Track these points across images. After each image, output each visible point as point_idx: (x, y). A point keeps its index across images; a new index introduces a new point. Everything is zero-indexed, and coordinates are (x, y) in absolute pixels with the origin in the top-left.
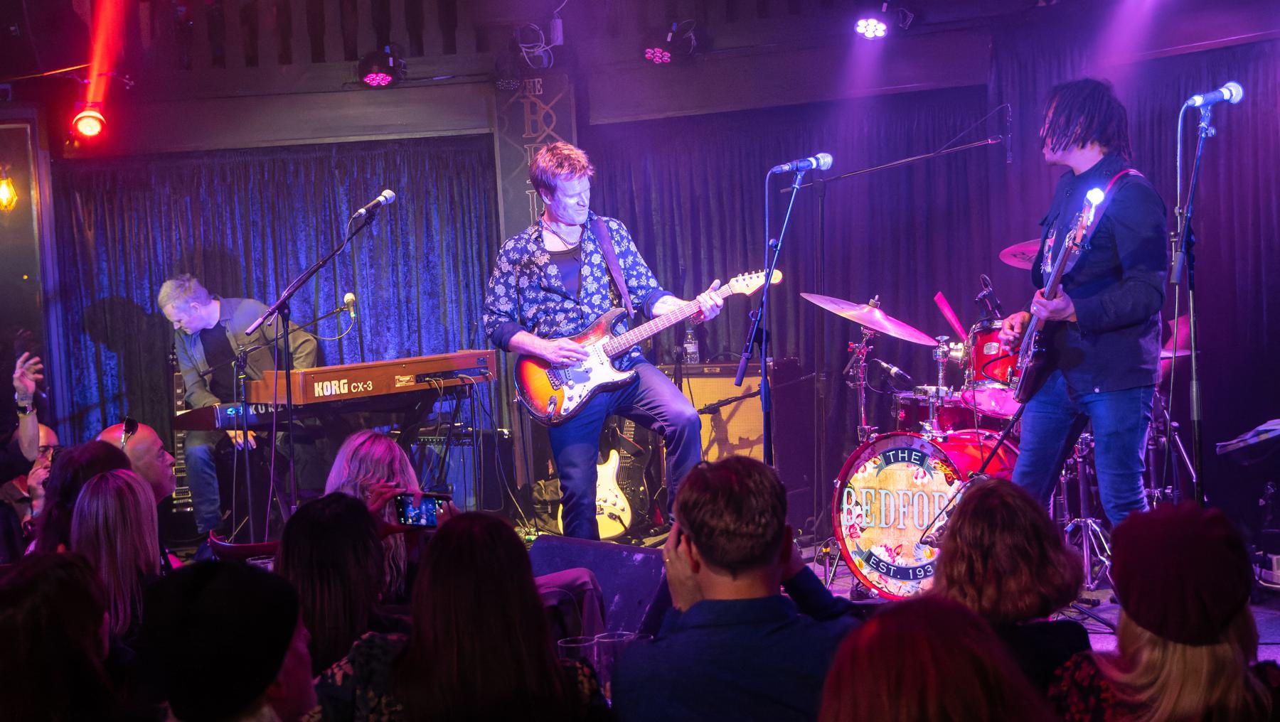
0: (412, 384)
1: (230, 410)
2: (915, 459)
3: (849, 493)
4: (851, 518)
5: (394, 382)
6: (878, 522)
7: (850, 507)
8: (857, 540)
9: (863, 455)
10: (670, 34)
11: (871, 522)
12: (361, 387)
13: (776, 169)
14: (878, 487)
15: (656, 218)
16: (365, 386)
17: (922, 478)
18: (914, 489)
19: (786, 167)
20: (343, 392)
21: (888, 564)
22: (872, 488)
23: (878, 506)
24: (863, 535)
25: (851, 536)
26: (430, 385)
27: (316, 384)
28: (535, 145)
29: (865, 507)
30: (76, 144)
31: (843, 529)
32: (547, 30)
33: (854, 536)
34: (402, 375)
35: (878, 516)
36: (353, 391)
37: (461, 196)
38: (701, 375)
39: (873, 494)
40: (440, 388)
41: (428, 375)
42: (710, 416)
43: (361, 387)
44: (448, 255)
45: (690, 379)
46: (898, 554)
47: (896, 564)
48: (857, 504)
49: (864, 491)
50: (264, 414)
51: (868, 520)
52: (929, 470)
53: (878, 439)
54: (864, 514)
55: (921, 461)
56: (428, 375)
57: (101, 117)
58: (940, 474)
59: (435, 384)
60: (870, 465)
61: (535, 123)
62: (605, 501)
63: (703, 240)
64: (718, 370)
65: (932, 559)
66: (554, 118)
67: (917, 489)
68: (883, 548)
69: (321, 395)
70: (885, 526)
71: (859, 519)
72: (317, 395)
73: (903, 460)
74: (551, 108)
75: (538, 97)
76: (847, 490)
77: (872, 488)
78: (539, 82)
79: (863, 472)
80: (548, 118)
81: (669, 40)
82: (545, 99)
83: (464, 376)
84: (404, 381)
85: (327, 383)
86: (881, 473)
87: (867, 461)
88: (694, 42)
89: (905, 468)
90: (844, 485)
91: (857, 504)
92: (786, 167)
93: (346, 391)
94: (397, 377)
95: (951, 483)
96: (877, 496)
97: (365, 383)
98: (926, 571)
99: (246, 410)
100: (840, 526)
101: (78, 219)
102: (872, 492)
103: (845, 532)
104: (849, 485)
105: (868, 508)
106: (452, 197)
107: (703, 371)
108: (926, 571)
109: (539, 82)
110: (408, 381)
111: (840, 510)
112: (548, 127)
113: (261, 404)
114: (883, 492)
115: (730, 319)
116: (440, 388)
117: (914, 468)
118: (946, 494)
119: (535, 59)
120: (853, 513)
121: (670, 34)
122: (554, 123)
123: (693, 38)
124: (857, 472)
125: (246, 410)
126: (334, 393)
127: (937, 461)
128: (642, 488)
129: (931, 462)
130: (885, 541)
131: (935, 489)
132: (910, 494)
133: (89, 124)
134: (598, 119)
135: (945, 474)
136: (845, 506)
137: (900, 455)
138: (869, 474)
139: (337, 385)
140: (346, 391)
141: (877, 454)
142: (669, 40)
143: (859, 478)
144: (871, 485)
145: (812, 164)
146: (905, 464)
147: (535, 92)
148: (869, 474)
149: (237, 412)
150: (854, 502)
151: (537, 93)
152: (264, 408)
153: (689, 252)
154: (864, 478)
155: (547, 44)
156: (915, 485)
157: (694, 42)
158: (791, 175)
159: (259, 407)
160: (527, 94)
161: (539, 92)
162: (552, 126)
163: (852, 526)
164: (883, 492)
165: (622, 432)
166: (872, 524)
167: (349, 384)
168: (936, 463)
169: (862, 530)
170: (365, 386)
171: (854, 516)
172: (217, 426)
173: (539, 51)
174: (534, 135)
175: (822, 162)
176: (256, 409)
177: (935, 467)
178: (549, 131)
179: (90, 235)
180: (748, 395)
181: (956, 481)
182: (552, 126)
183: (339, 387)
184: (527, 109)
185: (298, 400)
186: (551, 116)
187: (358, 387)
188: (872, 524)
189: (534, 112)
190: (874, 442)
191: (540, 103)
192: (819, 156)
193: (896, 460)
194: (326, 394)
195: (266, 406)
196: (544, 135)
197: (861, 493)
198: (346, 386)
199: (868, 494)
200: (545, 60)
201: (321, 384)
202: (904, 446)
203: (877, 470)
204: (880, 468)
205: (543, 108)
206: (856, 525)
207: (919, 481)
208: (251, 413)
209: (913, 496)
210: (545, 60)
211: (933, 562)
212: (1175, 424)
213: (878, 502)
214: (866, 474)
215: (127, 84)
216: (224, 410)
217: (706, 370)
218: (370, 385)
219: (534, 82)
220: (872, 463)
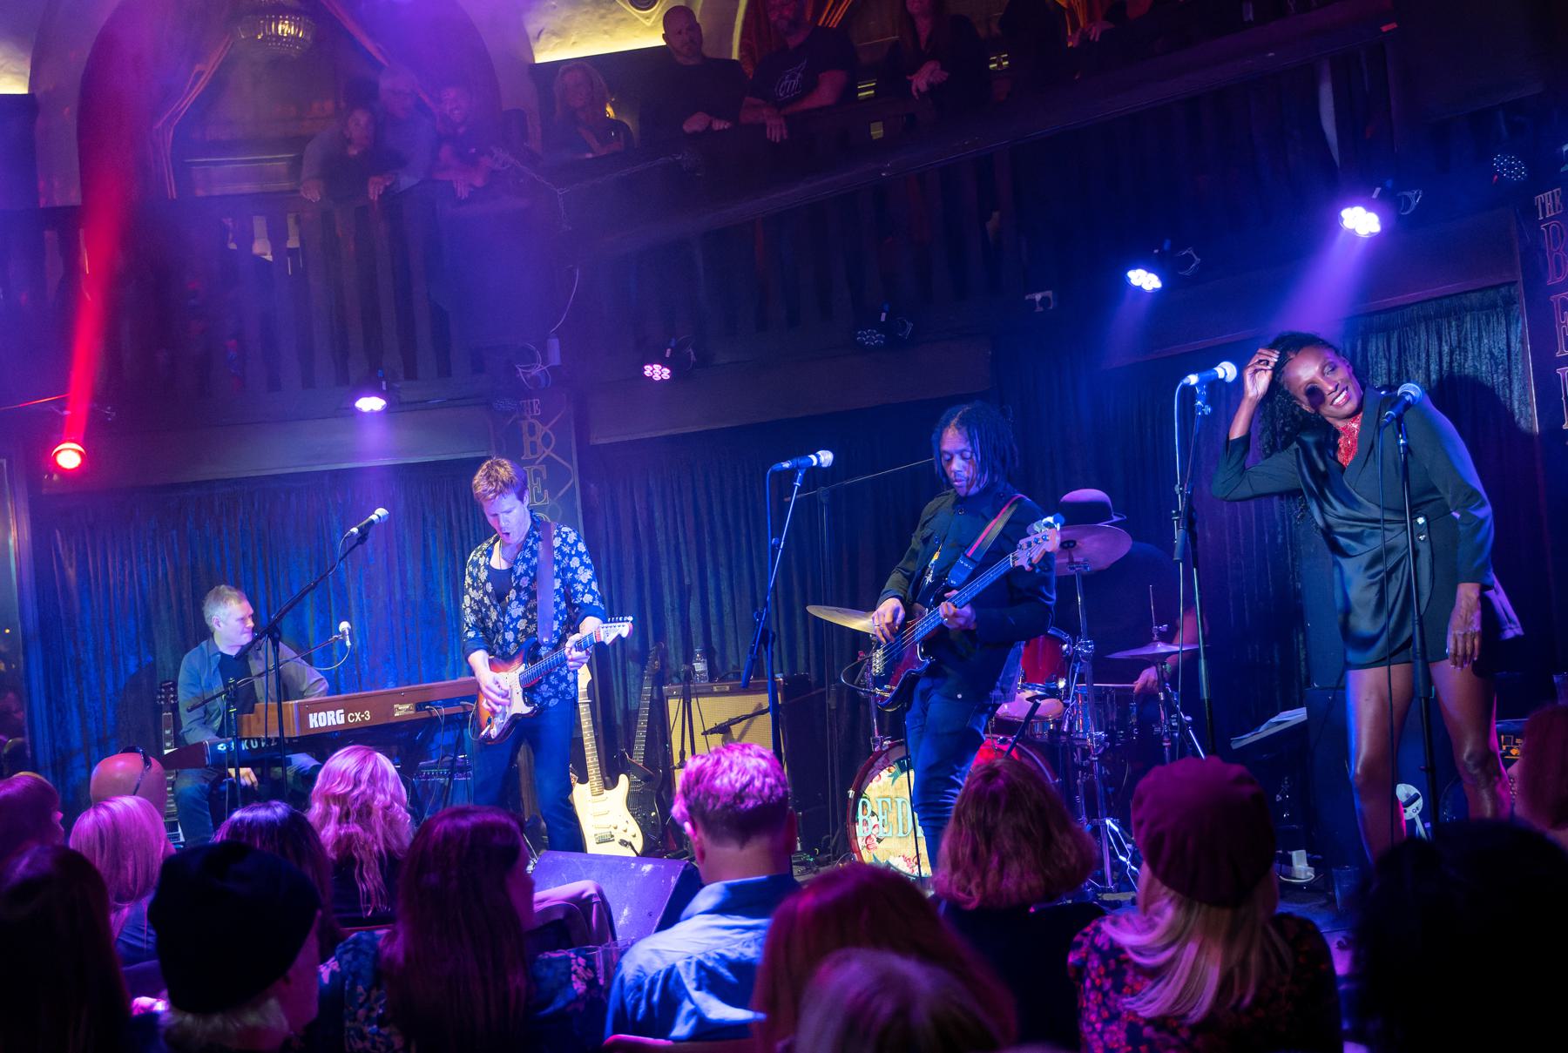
0: (412, 712)
1: (222, 745)
3: (864, 803)
4: (867, 829)
5: (393, 711)
6: (895, 832)
7: (866, 817)
8: (875, 852)
9: (876, 764)
10: (669, 350)
12: (358, 718)
13: (776, 467)
14: (892, 794)
15: (661, 538)
16: (363, 716)
19: (786, 465)
20: (339, 722)
22: (888, 797)
23: (895, 815)
24: (881, 846)
25: (867, 847)
26: (430, 712)
27: (311, 715)
28: (535, 467)
30: (55, 477)
31: (859, 840)
32: (544, 349)
33: (870, 847)
34: (402, 703)
35: (895, 826)
36: (349, 720)
37: (459, 521)
38: (711, 694)
40: (442, 716)
41: (429, 703)
42: (720, 736)
43: (358, 718)
44: (447, 582)
45: (699, 699)
48: (873, 814)
49: (880, 801)
50: (256, 749)
51: (885, 830)
53: (891, 746)
54: (880, 823)
56: (429, 703)
57: (82, 450)
59: (435, 712)
60: (885, 774)
61: (533, 444)
62: (616, 828)
63: (708, 557)
64: (728, 688)
66: (552, 435)
68: (901, 858)
69: (316, 726)
70: (902, 835)
71: (876, 829)
72: (312, 726)
74: (550, 429)
75: (536, 418)
76: (862, 800)
77: (888, 797)
78: (537, 402)
79: (877, 781)
80: (546, 438)
81: (668, 355)
82: (544, 419)
83: (466, 703)
84: (403, 710)
85: (322, 714)
86: (897, 781)
87: (882, 770)
88: (693, 358)
90: (859, 795)
91: (873, 814)
92: (786, 465)
93: (343, 722)
94: (395, 706)
96: (894, 805)
97: (362, 713)
99: (238, 746)
100: (856, 838)
101: (58, 557)
102: (888, 800)
103: (861, 843)
104: (864, 795)
105: (885, 817)
106: (450, 523)
107: (712, 689)
109: (537, 402)
110: (407, 710)
111: (855, 821)
112: (547, 448)
113: (253, 739)
114: (899, 801)
115: (739, 637)
116: (442, 716)
119: (535, 380)
120: (869, 822)
121: (669, 350)
122: (553, 443)
123: (692, 353)
124: (871, 781)
125: (238, 746)
126: (329, 724)
128: (653, 814)
130: (902, 853)
133: (69, 457)
134: (598, 439)
136: (860, 817)
138: (884, 783)
139: (333, 716)
140: (343, 722)
141: (891, 763)
142: (668, 355)
143: (873, 788)
144: (887, 794)
145: (812, 462)
147: (532, 411)
148: (884, 783)
149: (229, 749)
150: (869, 812)
151: (535, 414)
152: (256, 743)
153: (695, 572)
154: (879, 787)
155: (544, 363)
157: (693, 358)
158: (791, 473)
159: (252, 742)
160: (526, 414)
161: (537, 412)
162: (552, 446)
163: (869, 837)
164: (899, 801)
165: (631, 756)
166: (890, 834)
167: (346, 714)
169: (879, 840)
170: (363, 716)
171: (870, 827)
172: (207, 763)
173: (534, 372)
174: (533, 457)
175: (822, 459)
176: (249, 744)
178: (548, 452)
179: (71, 573)
180: (760, 712)
182: (552, 446)
183: (335, 717)
184: (525, 428)
185: (292, 731)
186: (551, 439)
187: (355, 717)
188: (890, 834)
189: (532, 431)
190: (887, 750)
191: (538, 426)
192: (819, 453)
194: (323, 724)
195: (259, 740)
196: (544, 456)
198: (343, 716)
199: (885, 805)
200: (543, 381)
201: (315, 714)
203: (892, 778)
204: (895, 777)
205: (541, 429)
206: (873, 836)
208: (243, 748)
210: (543, 381)
212: (1189, 718)
213: (894, 811)
214: (881, 783)
215: (109, 416)
216: (214, 745)
217: (715, 689)
218: (368, 715)
219: (532, 403)
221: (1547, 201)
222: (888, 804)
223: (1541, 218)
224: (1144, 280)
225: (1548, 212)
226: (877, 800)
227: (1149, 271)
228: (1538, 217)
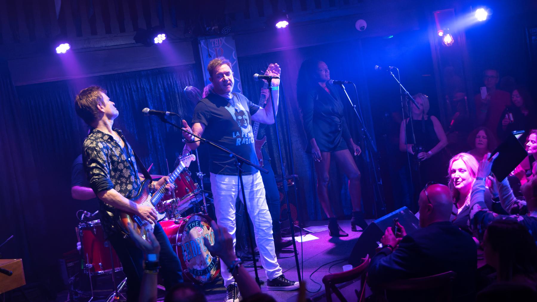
2: (197, 224)
11: (191, 256)
17: (201, 231)
18: (200, 236)
21: (200, 271)
22: (187, 242)
29: (187, 251)
39: (189, 244)
46: (201, 265)
47: (202, 269)
48: (185, 251)
49: (185, 244)
52: (202, 227)
54: (188, 254)
55: (199, 225)
58: (205, 228)
65: (211, 261)
67: (200, 236)
73: (194, 226)
77: (187, 242)
89: (195, 229)
95: (209, 229)
98: (211, 267)
102: (188, 243)
108: (211, 267)
117: (198, 228)
118: (208, 234)
127: (203, 222)
129: (202, 223)
131: (205, 233)
132: (199, 239)
135: (207, 226)
137: (193, 225)
144: (187, 241)
146: (195, 227)
156: (199, 235)
168: (203, 223)
169: (189, 261)
177: (203, 225)
181: (210, 228)
188: (191, 257)
193: (192, 227)
197: (185, 245)
202: (193, 220)
203: (187, 234)
206: (187, 260)
207: (200, 233)
209: (200, 239)
211: (212, 262)
220: (185, 232)
221: (216, 41)
222: (188, 244)
223: (213, 46)
224: (63, 48)
225: (216, 44)
226: (185, 244)
227: (58, 46)
228: (212, 45)
